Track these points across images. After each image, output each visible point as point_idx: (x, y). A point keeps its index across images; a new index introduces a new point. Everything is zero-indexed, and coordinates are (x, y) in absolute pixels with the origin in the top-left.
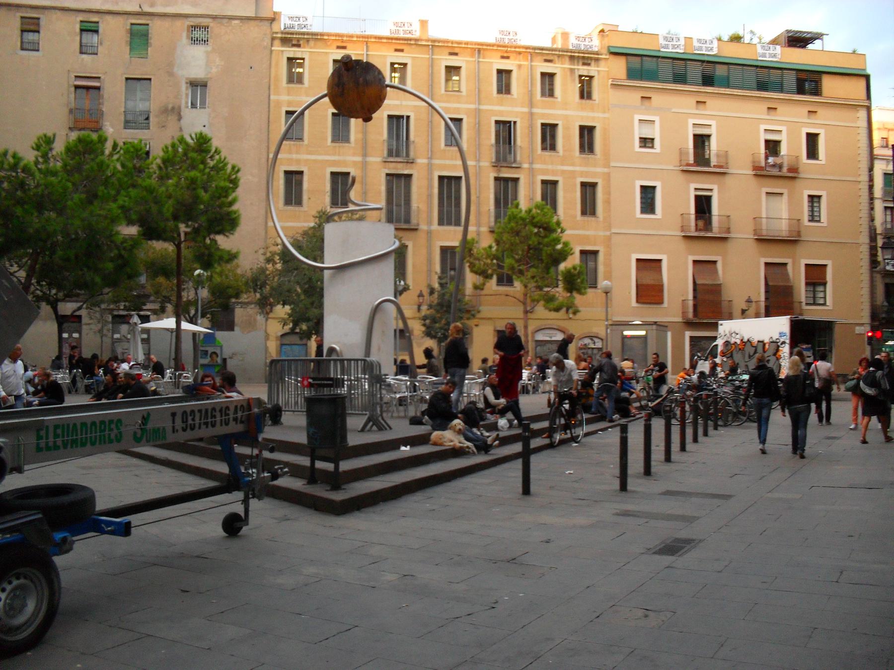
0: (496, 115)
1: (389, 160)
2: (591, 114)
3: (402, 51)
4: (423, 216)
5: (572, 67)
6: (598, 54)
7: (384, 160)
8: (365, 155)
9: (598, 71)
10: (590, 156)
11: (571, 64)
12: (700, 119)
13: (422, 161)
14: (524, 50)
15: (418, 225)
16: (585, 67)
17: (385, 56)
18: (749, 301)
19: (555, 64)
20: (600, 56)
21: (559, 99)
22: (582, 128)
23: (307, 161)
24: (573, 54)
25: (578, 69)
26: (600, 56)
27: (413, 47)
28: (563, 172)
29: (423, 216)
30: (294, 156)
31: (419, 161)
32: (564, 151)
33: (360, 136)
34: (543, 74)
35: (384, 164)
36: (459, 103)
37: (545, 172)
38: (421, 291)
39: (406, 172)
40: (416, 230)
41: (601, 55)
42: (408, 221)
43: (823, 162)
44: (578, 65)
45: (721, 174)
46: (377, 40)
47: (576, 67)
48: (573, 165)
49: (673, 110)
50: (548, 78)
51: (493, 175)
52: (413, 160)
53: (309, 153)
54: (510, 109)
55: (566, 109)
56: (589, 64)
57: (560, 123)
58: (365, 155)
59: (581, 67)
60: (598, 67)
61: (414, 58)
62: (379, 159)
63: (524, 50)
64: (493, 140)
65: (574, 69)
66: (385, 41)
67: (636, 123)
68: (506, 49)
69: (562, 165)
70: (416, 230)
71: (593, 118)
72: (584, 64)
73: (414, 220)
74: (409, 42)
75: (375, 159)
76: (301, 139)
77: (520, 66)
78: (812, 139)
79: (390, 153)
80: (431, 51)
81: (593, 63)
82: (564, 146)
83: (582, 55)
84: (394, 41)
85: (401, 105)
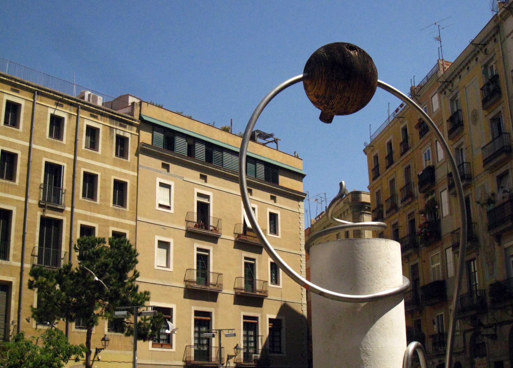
0: (47, 157)
2: (124, 171)
5: (112, 126)
6: (133, 120)
9: (131, 134)
10: (121, 208)
11: (111, 123)
12: (202, 189)
14: (75, 102)
16: (122, 128)
18: (237, 348)
19: (98, 120)
20: (134, 122)
21: (100, 152)
22: (116, 182)
24: (113, 115)
25: (116, 129)
26: (134, 122)
28: (99, 220)
32: (101, 200)
34: (89, 128)
36: (16, 138)
37: (85, 218)
41: (135, 120)
43: (279, 237)
44: (116, 125)
45: (214, 239)
47: (115, 127)
48: (107, 214)
49: (184, 179)
50: (92, 132)
51: (39, 213)
54: (58, 153)
55: (105, 163)
56: (125, 127)
57: (99, 174)
59: (118, 128)
60: (131, 130)
63: (75, 102)
64: (42, 181)
65: (113, 128)
67: (158, 184)
68: (61, 97)
69: (99, 213)
71: (125, 175)
72: (121, 125)
77: (70, 115)
78: (273, 217)
81: (128, 126)
82: (101, 196)
83: (120, 117)
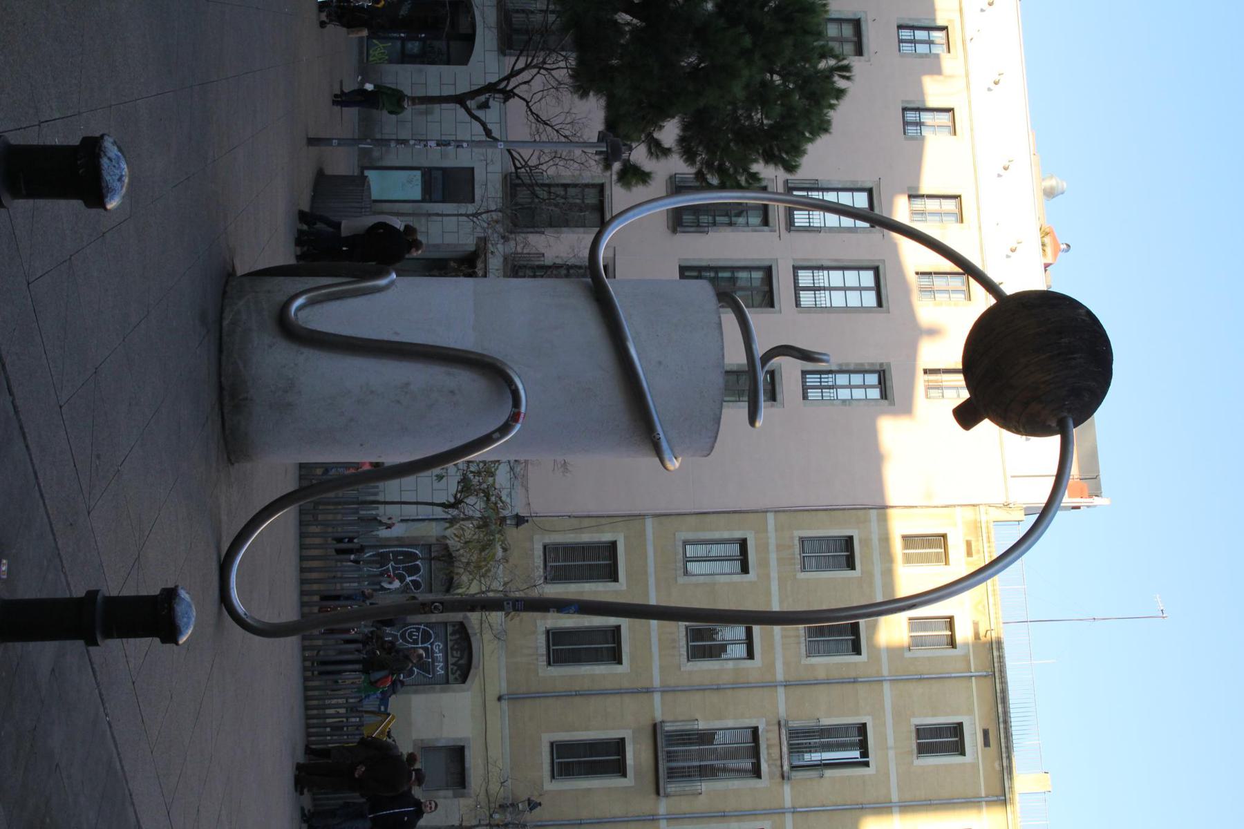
1: (783, 731)
3: (987, 743)
4: (684, 805)
7: (783, 723)
8: (787, 685)
13: (787, 794)
15: (667, 796)
17: (970, 711)
23: (768, 576)
27: (997, 766)
29: (684, 805)
30: (773, 556)
31: (787, 789)
33: (822, 675)
35: (775, 721)
38: (540, 804)
39: (764, 767)
40: (658, 793)
42: (673, 774)
46: (998, 695)
52: (789, 779)
53: (782, 581)
58: (787, 685)
61: (975, 766)
62: (782, 711)
66: (1000, 710)
70: (658, 793)
73: (672, 788)
74: (1004, 755)
75: (781, 704)
76: (803, 569)
79: (794, 733)
80: (995, 798)
84: (1002, 726)
85: (887, 748)
